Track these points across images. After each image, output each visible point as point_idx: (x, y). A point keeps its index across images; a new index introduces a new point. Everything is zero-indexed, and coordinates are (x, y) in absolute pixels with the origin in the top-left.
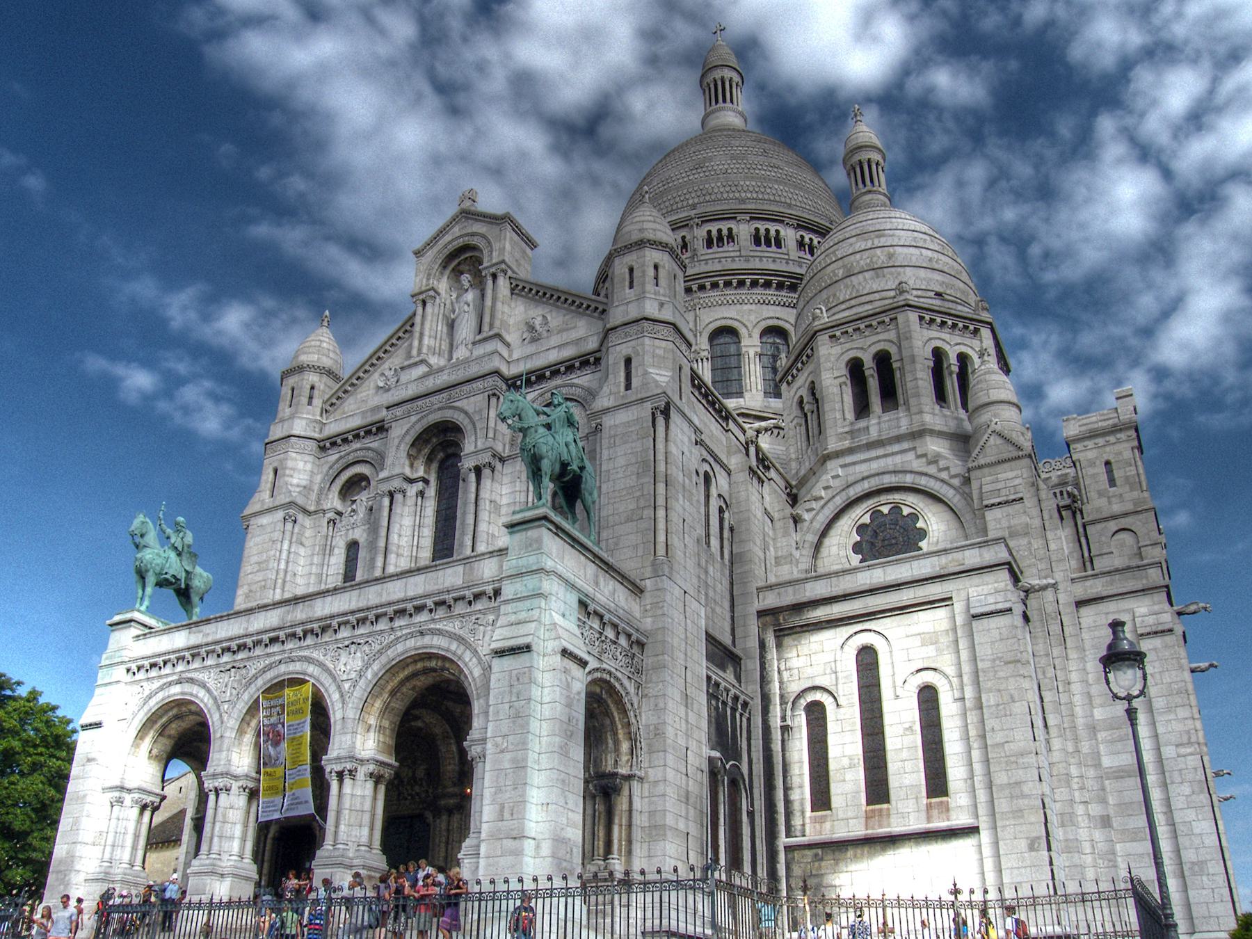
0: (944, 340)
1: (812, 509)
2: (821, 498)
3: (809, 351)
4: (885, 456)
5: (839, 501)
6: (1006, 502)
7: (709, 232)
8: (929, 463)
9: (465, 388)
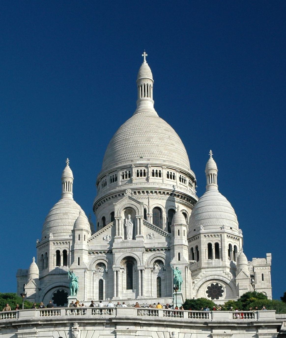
0: (231, 242)
1: (197, 281)
2: (199, 278)
3: (197, 237)
4: (216, 271)
5: (204, 280)
6: (244, 289)
7: (153, 170)
8: (226, 275)
9: (135, 249)
